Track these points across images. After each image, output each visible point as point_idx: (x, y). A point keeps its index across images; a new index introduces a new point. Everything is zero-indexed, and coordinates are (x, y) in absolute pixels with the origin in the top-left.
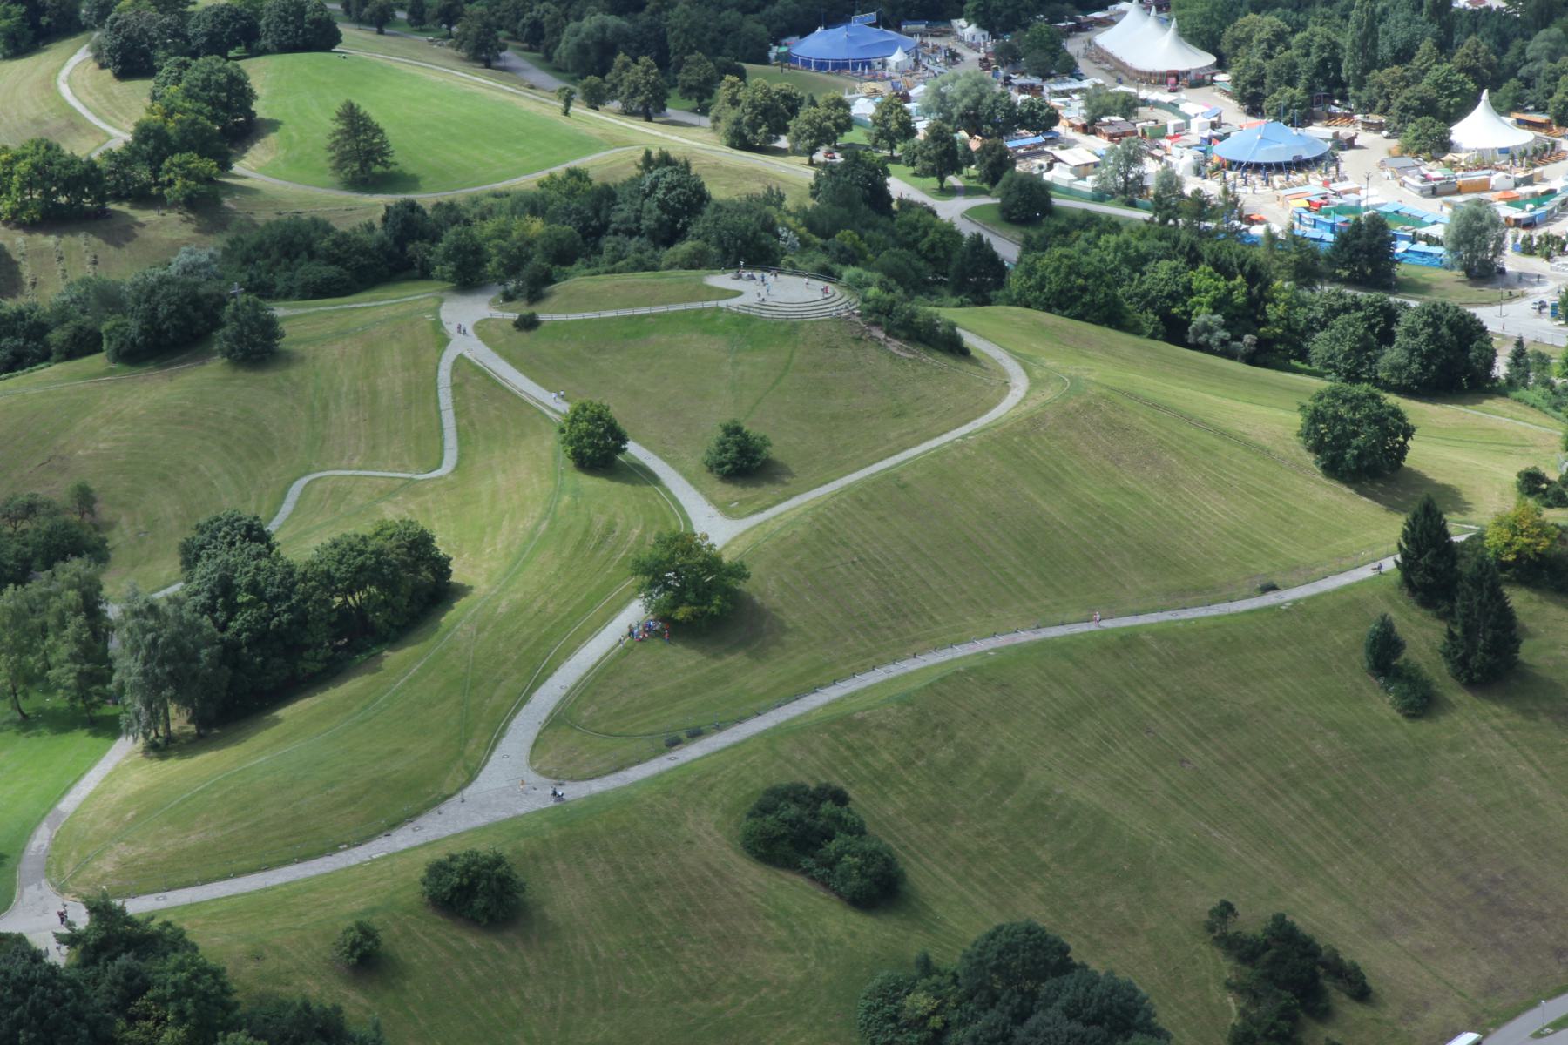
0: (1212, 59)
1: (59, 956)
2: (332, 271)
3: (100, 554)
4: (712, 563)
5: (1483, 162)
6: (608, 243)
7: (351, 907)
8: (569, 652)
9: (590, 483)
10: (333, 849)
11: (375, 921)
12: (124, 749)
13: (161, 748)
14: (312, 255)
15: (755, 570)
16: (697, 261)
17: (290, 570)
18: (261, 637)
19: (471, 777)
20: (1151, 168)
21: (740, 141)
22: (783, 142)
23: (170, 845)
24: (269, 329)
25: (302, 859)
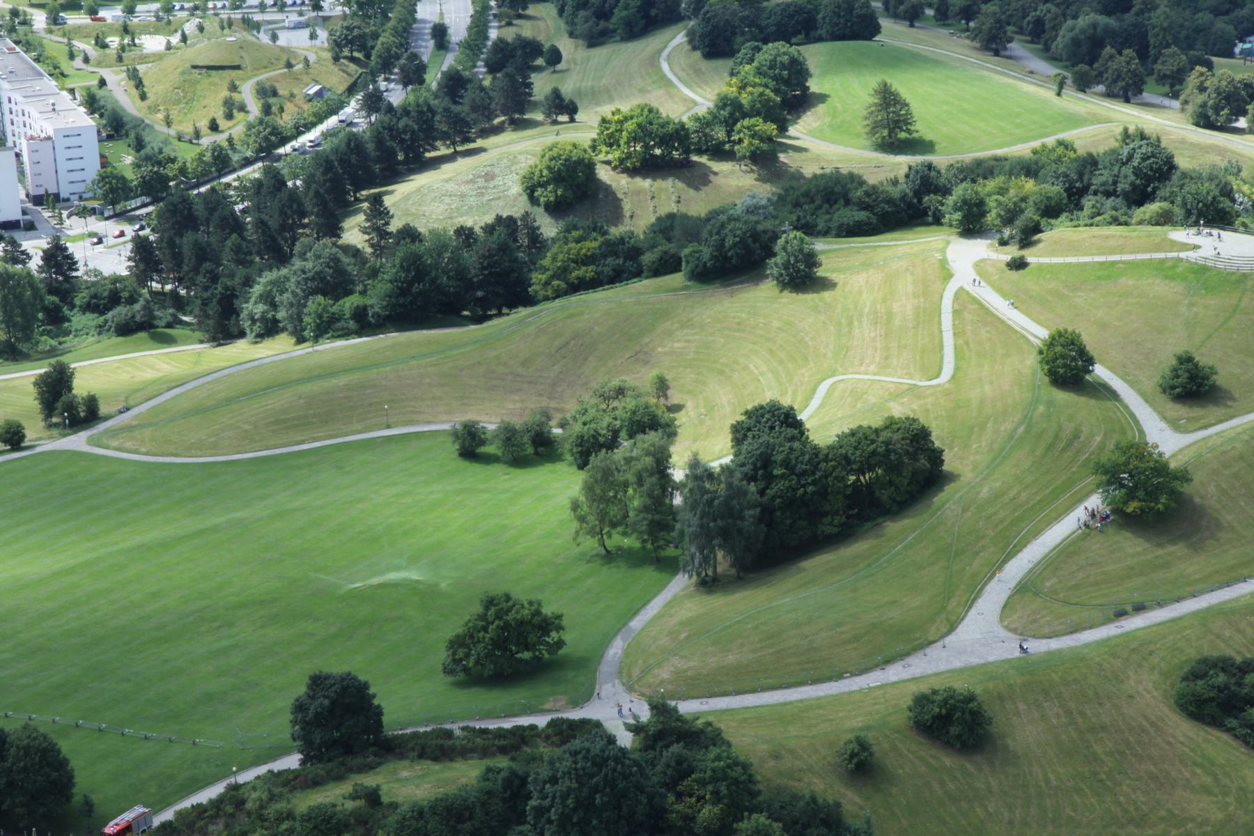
1: (625, 739)
2: (862, 215)
3: (670, 432)
4: (1161, 468)
6: (1088, 202)
7: (853, 723)
8: (1036, 533)
9: (1062, 396)
10: (839, 676)
11: (870, 737)
12: (681, 583)
13: (709, 584)
14: (848, 202)
15: (1198, 477)
16: (1165, 219)
17: (815, 447)
18: (791, 503)
19: (952, 628)
21: (1205, 121)
22: (1242, 123)
23: (713, 662)
24: (811, 260)
25: (815, 681)
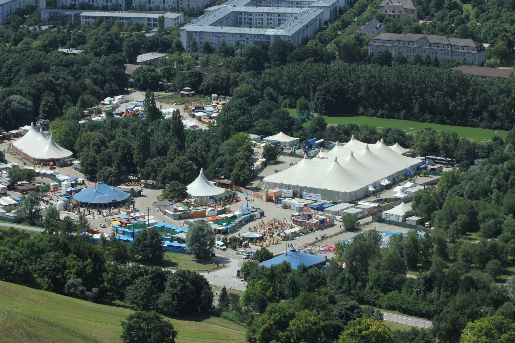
0: (70, 153)
5: (202, 201)
20: (43, 206)
